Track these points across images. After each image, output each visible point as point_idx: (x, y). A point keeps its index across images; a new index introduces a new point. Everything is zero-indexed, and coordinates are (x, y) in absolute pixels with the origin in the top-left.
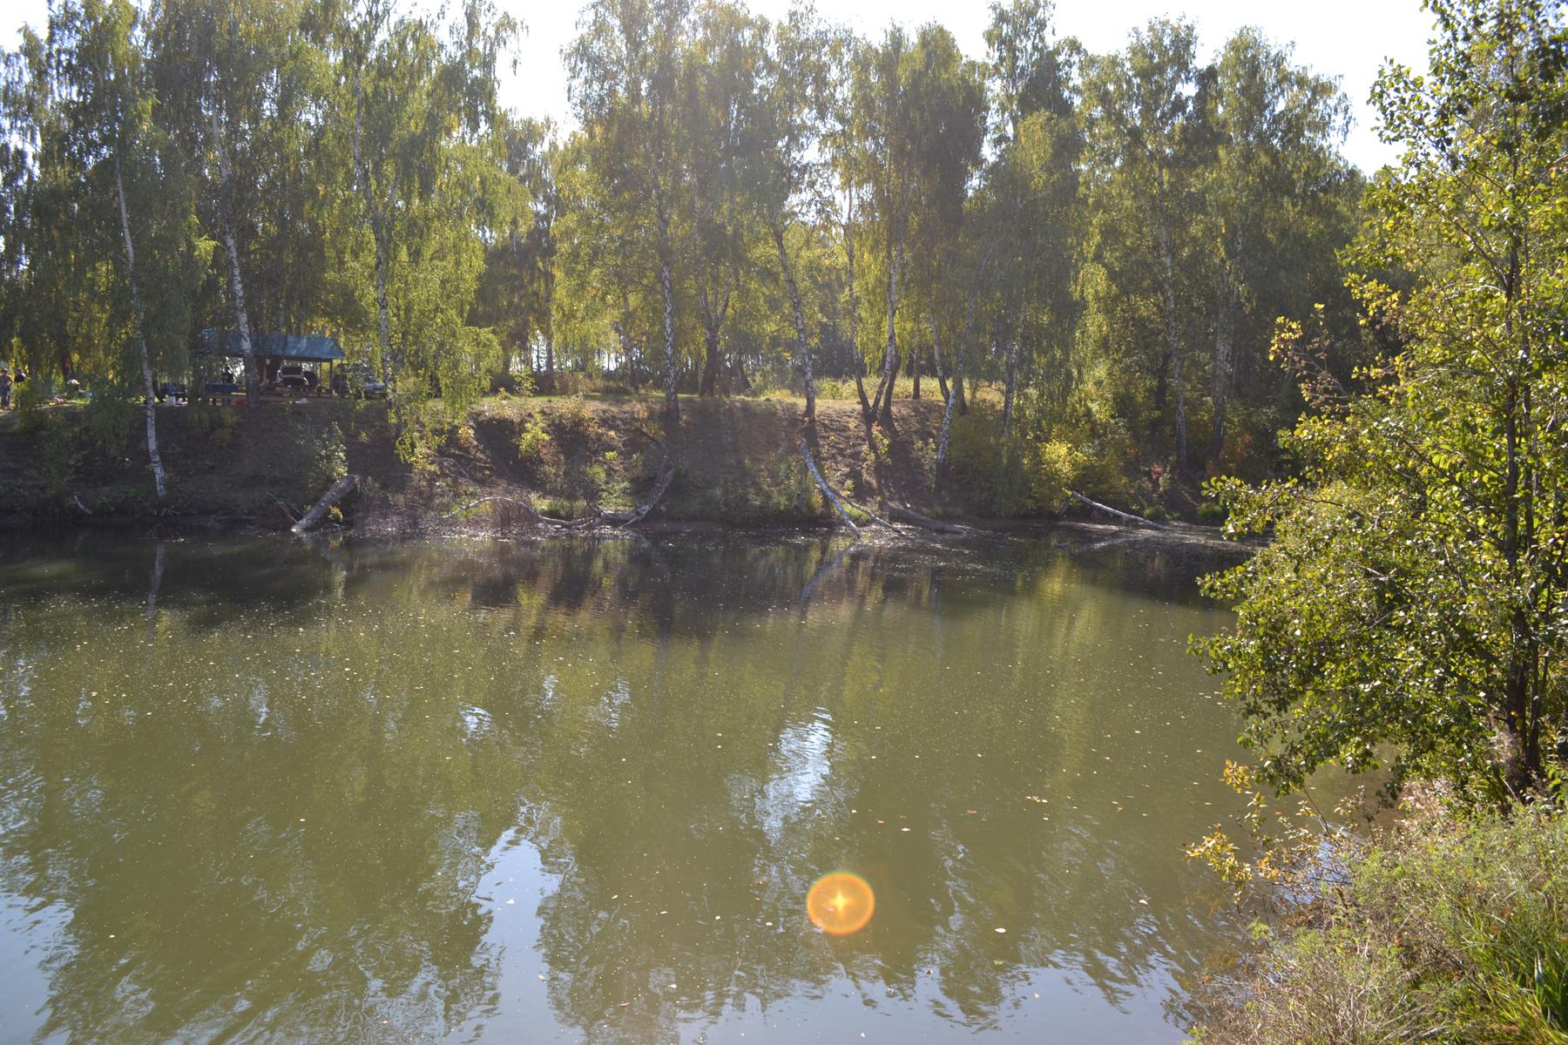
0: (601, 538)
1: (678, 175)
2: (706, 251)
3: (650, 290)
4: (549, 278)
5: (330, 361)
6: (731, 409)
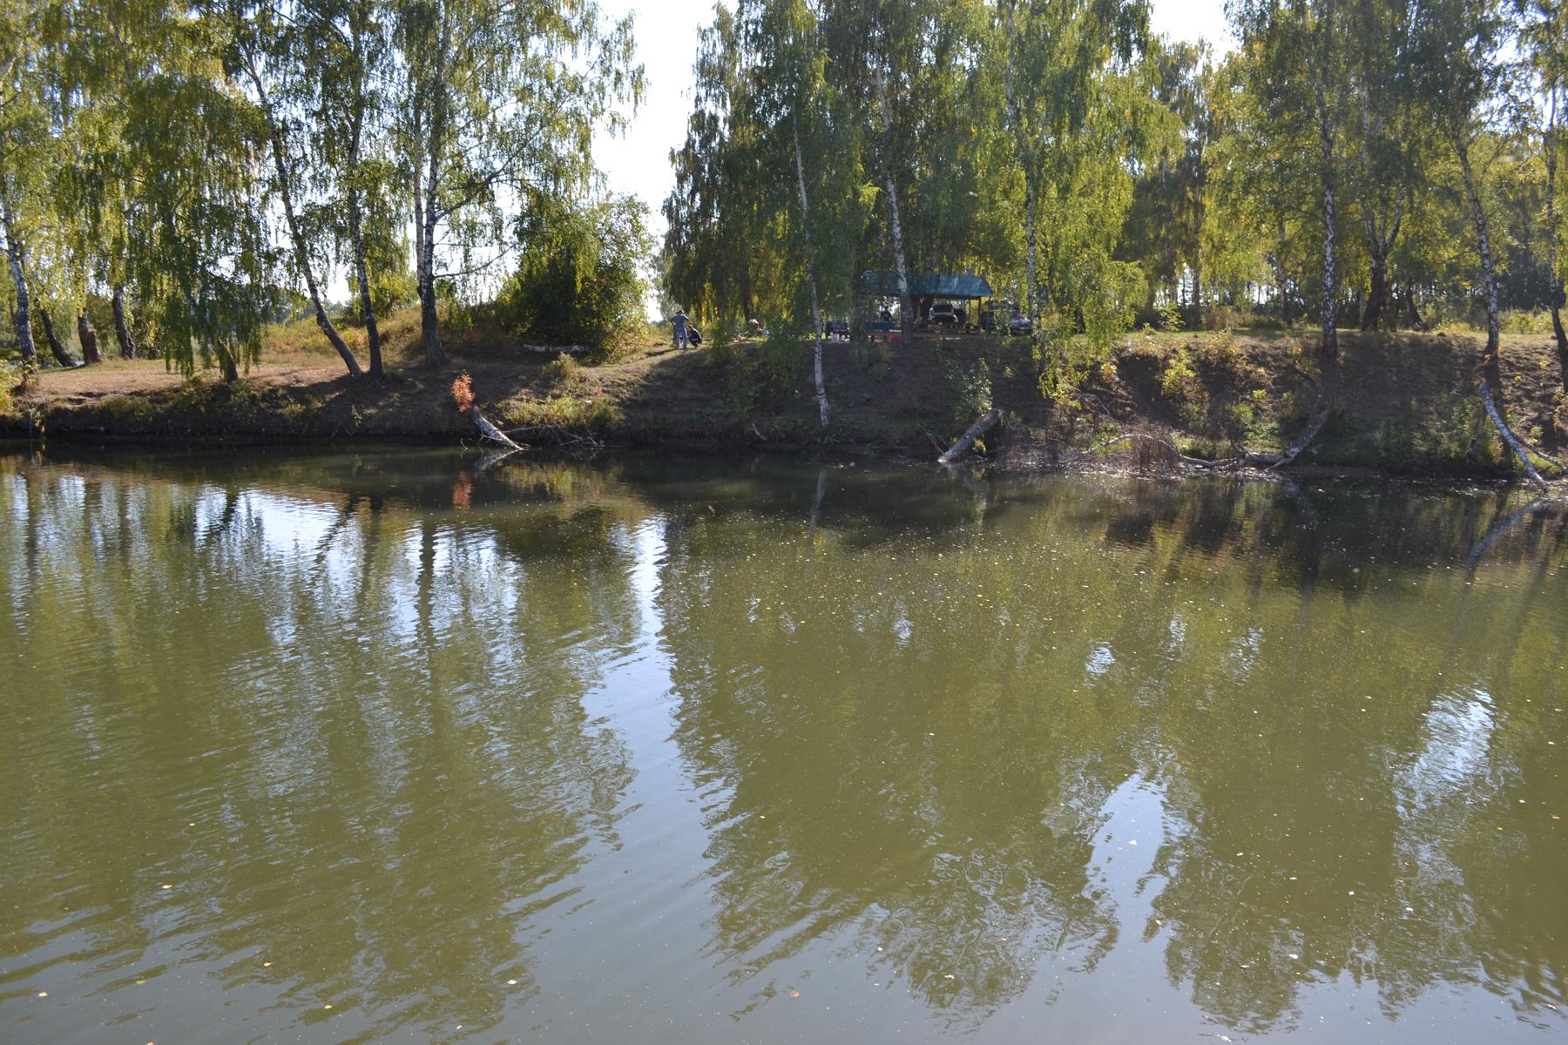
0: (1245, 480)
1: (1346, 89)
2: (1377, 172)
3: (1311, 217)
4: (1199, 208)
5: (978, 298)
6: (1397, 344)
